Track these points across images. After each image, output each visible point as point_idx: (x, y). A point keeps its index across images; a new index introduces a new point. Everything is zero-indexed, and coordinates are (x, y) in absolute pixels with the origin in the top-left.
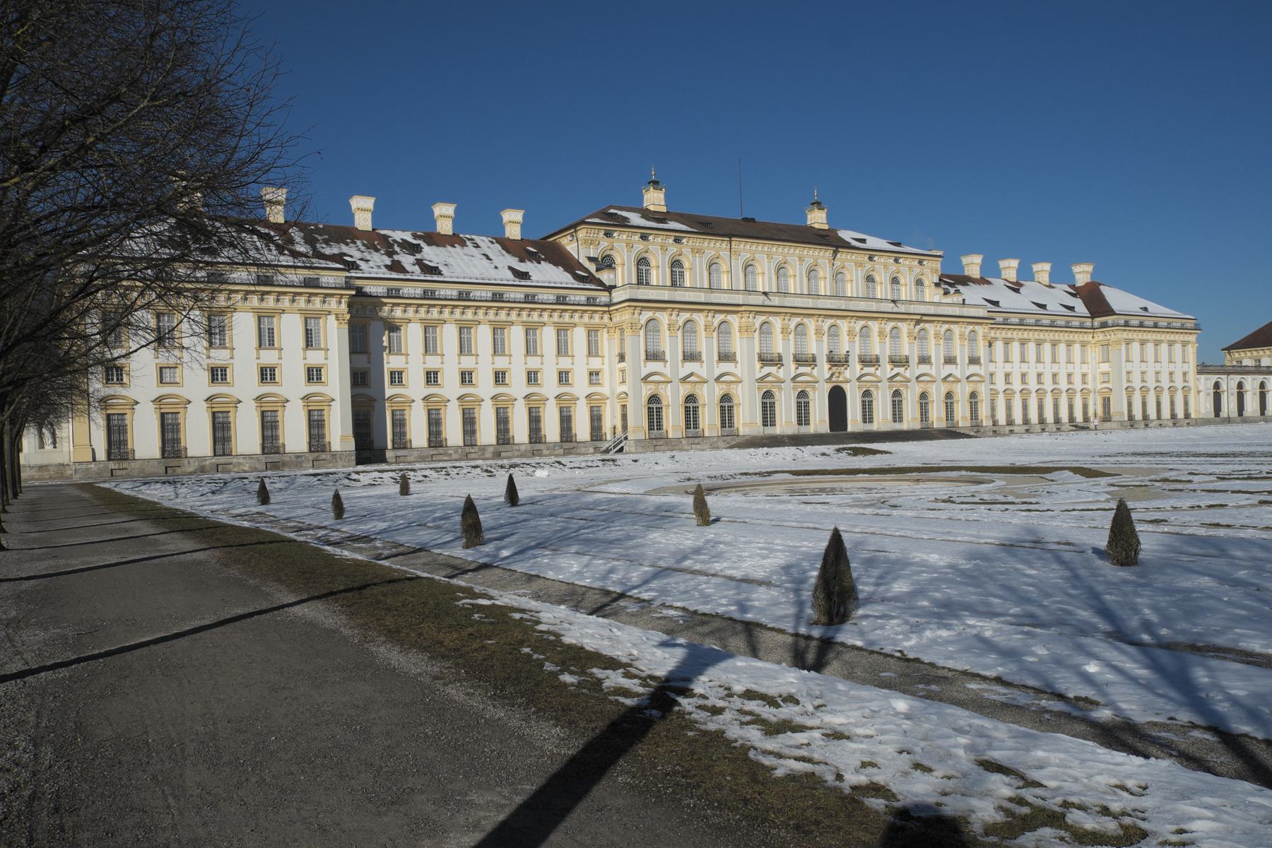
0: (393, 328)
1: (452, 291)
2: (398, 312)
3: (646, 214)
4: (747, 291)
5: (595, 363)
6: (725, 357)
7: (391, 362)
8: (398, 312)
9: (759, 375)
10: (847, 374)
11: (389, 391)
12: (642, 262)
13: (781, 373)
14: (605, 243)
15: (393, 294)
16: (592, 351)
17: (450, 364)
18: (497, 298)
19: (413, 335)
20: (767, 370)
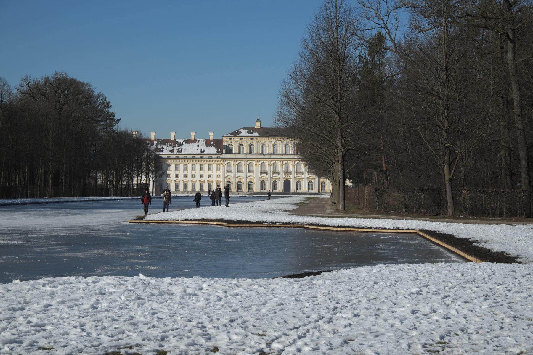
0: (169, 165)
1: (182, 156)
2: (169, 162)
3: (251, 130)
4: (262, 154)
5: (218, 173)
6: (250, 171)
7: (168, 172)
8: (169, 162)
9: (260, 176)
10: (291, 176)
11: (168, 179)
12: (240, 146)
13: (267, 176)
14: (229, 141)
15: (168, 158)
16: (218, 169)
17: (181, 173)
18: (193, 158)
19: (173, 166)
20: (262, 175)
